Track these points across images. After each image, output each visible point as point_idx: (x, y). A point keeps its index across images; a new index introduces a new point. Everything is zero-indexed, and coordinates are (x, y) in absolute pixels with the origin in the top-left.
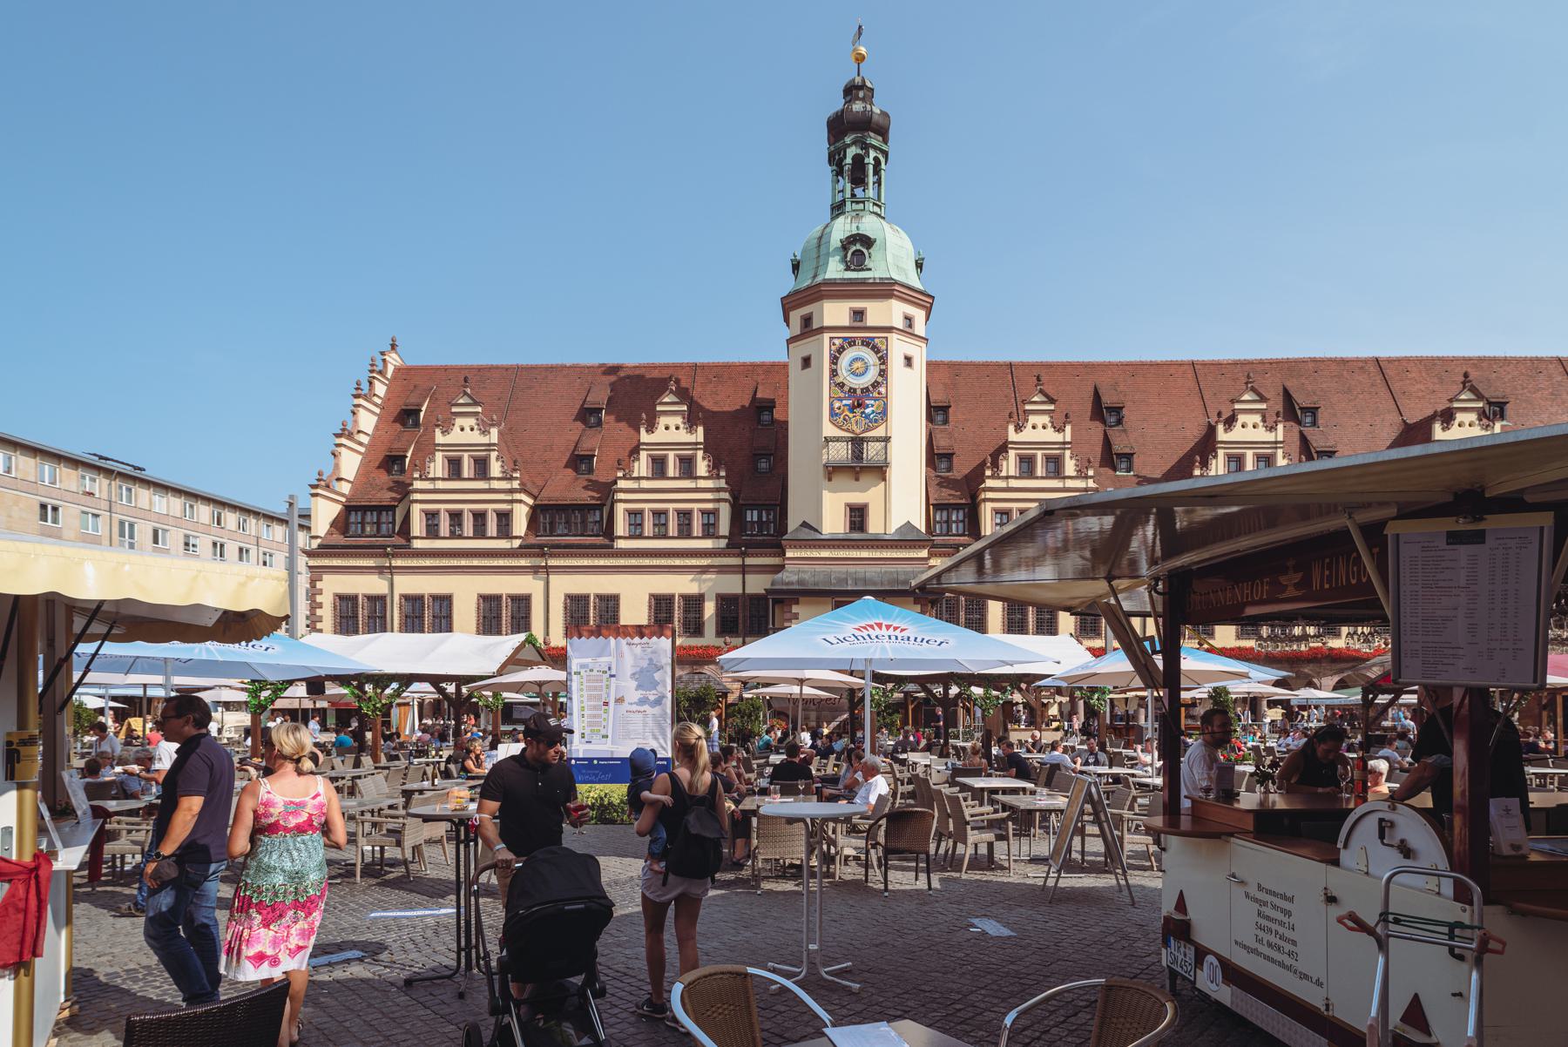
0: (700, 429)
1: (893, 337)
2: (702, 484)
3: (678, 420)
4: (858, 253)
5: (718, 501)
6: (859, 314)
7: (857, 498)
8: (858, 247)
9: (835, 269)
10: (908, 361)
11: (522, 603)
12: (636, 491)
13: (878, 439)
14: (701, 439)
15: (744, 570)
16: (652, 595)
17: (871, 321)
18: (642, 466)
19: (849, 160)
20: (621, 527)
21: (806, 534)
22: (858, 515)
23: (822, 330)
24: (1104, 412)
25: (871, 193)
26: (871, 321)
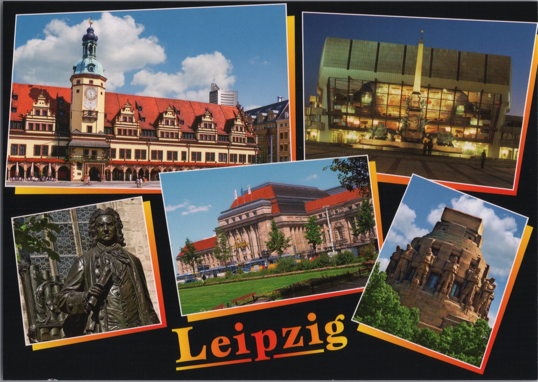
1: (99, 88)
2: (49, 118)
3: (43, 101)
4: (91, 68)
6: (91, 82)
7: (90, 124)
8: (92, 67)
9: (86, 71)
10: (102, 93)
15: (59, 140)
17: (94, 83)
18: (33, 113)
20: (27, 127)
21: (77, 132)
24: (139, 108)
26: (94, 83)
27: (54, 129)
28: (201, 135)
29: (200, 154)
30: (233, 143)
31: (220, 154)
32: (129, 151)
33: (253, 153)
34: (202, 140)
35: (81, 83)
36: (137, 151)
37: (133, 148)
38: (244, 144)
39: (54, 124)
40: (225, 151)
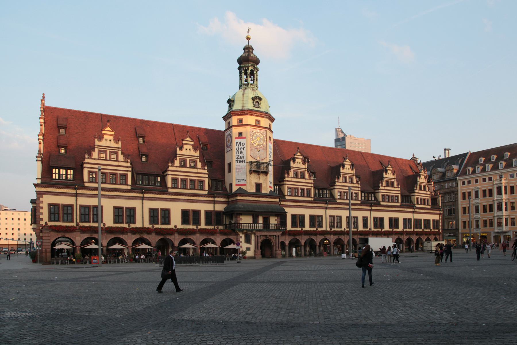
0: (198, 151)
3: (191, 147)
5: (205, 177)
9: (250, 105)
11: (132, 211)
12: (175, 171)
13: (264, 163)
14: (199, 155)
15: (214, 202)
16: (182, 210)
19: (249, 71)
22: (258, 186)
23: (247, 125)
25: (255, 82)
27: (207, 187)
28: (382, 195)
29: (382, 219)
30: (417, 206)
31: (405, 220)
32: (302, 217)
33: (437, 217)
34: (384, 201)
35: (244, 123)
36: (312, 217)
37: (307, 213)
38: (429, 207)
39: (207, 180)
40: (409, 216)
